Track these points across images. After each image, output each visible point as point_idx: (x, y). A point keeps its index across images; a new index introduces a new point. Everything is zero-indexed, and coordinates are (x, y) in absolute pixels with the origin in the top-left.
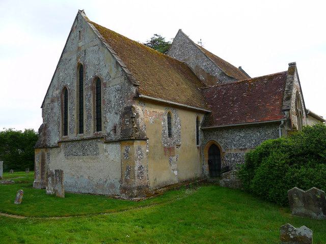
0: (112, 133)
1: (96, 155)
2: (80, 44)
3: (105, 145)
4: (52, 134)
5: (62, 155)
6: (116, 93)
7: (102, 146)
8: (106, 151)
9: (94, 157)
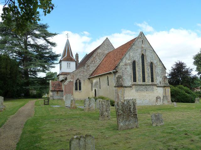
0: (159, 84)
2: (143, 46)
3: (156, 88)
4: (126, 80)
7: (155, 88)
9: (152, 92)
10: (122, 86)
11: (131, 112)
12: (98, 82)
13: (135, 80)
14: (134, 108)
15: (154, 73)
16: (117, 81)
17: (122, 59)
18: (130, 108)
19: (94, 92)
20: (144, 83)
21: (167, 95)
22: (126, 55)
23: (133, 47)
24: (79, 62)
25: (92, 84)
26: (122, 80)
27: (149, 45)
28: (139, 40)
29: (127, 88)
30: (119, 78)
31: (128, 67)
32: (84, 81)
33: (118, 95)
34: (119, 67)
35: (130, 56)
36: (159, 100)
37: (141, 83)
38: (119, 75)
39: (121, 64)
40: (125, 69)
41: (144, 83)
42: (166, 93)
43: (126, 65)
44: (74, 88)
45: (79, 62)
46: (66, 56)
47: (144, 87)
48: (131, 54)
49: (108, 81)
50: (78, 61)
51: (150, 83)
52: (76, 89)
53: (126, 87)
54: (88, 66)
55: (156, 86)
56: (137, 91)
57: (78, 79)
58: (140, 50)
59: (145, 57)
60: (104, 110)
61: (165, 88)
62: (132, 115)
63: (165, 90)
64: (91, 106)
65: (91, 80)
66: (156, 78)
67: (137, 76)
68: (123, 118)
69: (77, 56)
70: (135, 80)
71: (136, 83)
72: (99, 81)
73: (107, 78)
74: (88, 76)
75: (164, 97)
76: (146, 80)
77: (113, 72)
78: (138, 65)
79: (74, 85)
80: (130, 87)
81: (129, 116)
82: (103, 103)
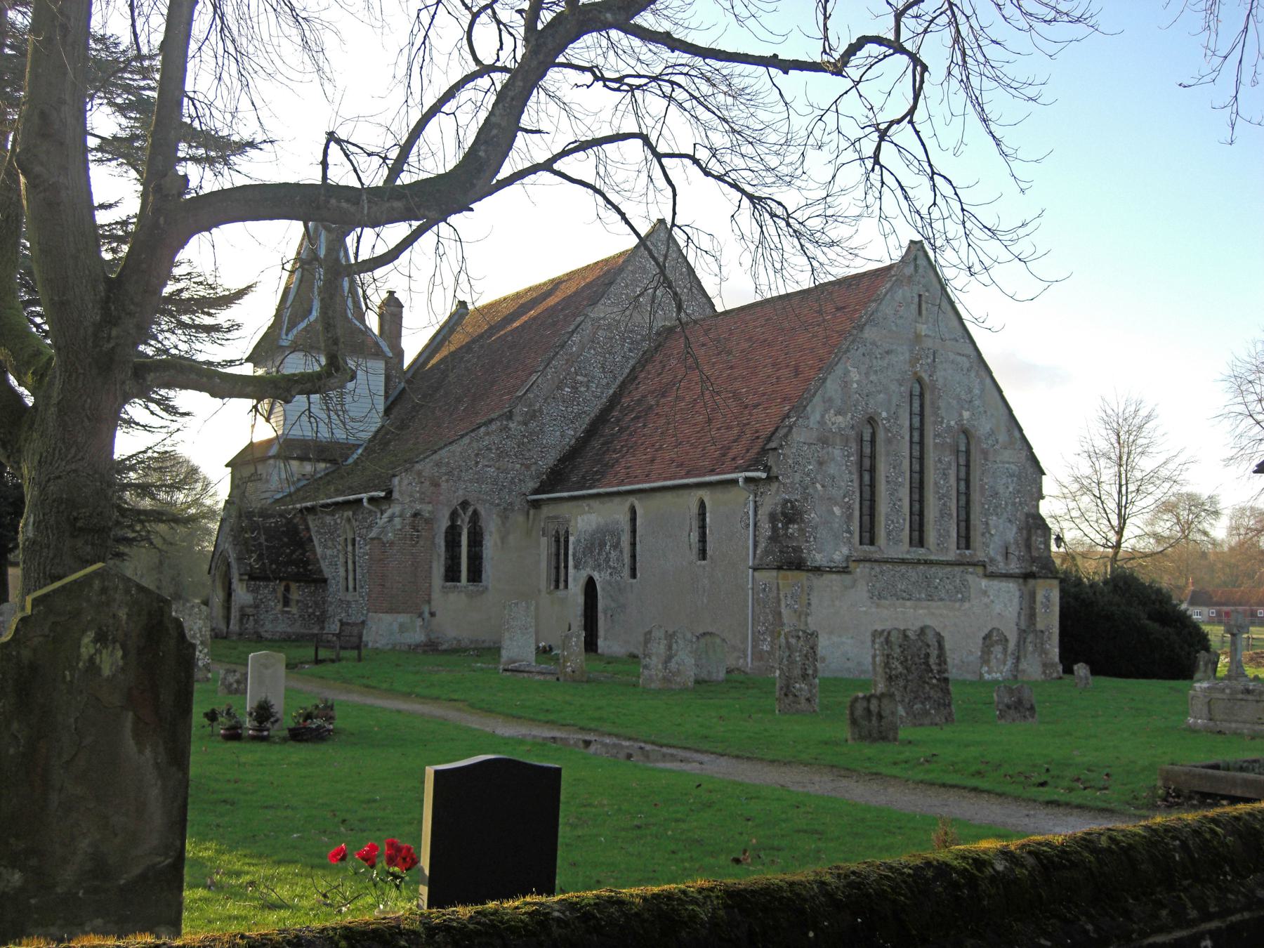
0: (999, 558)
1: (962, 600)
2: (923, 329)
3: (984, 583)
5: (862, 591)
6: (1010, 480)
7: (979, 583)
8: (985, 593)
9: (957, 605)
10: (797, 564)
11: (931, 671)
12: (616, 534)
13: (869, 534)
14: (939, 657)
15: (976, 497)
16: (774, 538)
17: (800, 408)
18: (927, 655)
19: (581, 600)
20: (920, 553)
21: (1040, 625)
22: (824, 380)
23: (869, 333)
24: (408, 360)
25: (560, 541)
26: (801, 530)
27: (955, 323)
28: (899, 294)
29: (828, 578)
30: (790, 515)
31: (837, 452)
32: (504, 516)
33: (780, 613)
34: (786, 451)
35: (846, 384)
36: (997, 649)
37: (903, 550)
38: (787, 501)
39: (799, 436)
40: (821, 463)
41: (920, 553)
42: (1032, 616)
43: (824, 441)
44: (438, 569)
45: (408, 360)
46: (315, 314)
47: (913, 574)
48: (854, 375)
49: (703, 527)
50: (400, 354)
51: (952, 554)
52: (452, 574)
53: (818, 570)
54: (533, 415)
55: (980, 570)
56: (877, 596)
57: (465, 504)
58: (902, 357)
59: (927, 397)
60: (797, 672)
61: (1031, 582)
62: (934, 681)
63: (1033, 596)
64: (673, 665)
65: (546, 511)
66: (987, 524)
67: (883, 508)
68: (905, 688)
69: (392, 309)
70: (869, 534)
71: (872, 548)
72: (627, 527)
73: (695, 509)
74: (532, 485)
75: (1022, 634)
76: (931, 536)
77: (747, 480)
78: (889, 441)
79: (441, 542)
80: (845, 571)
81: (925, 682)
82: (793, 641)
